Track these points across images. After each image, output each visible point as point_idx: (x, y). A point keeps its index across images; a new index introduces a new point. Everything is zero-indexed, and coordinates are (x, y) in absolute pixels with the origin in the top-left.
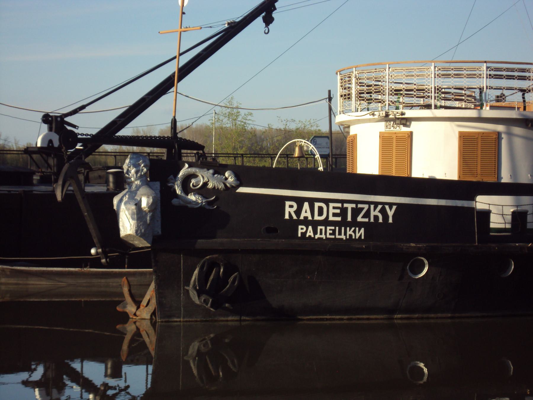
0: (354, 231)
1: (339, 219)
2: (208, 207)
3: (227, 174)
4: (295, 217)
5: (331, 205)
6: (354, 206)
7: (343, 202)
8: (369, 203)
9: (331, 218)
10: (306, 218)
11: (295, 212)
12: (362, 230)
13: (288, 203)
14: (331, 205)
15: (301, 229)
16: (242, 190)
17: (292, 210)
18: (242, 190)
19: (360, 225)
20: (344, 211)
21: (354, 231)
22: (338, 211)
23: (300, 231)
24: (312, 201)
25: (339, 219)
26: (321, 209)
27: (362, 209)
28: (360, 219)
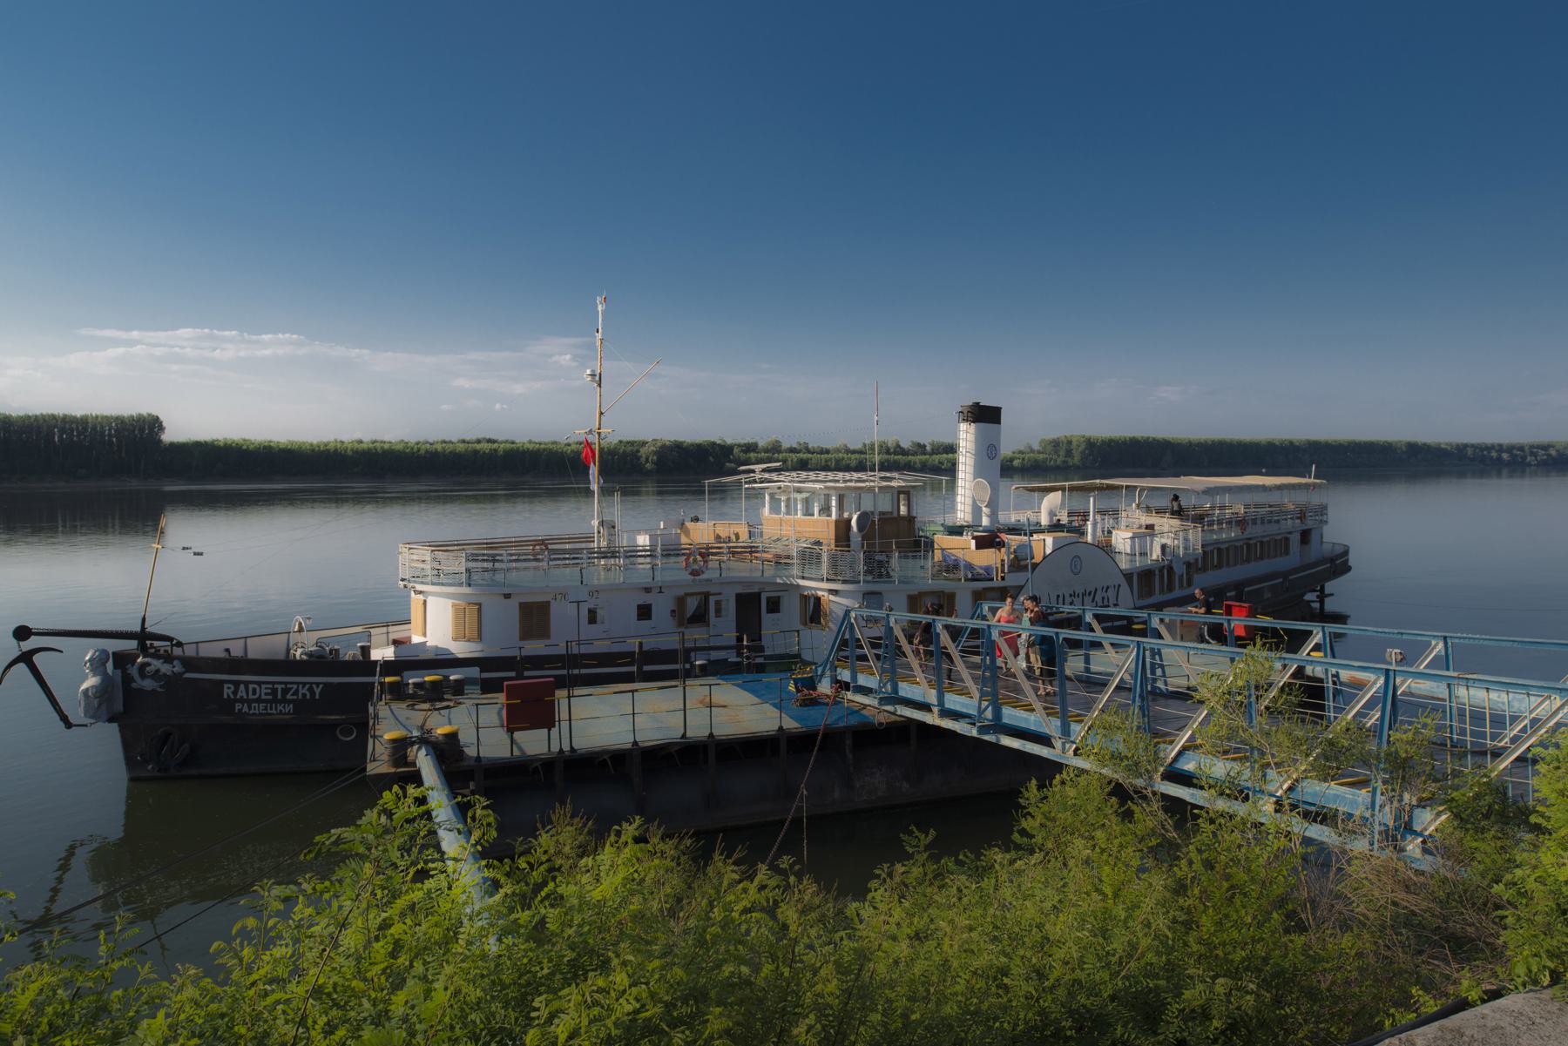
0: (284, 707)
1: (270, 697)
2: (159, 690)
3: (175, 662)
4: (232, 697)
5: (263, 686)
6: (283, 686)
7: (273, 683)
8: (298, 683)
9: (263, 697)
10: (242, 697)
11: (233, 693)
12: (291, 706)
13: (226, 686)
14: (263, 686)
15: (238, 706)
16: (187, 675)
17: (230, 691)
18: (187, 675)
19: (289, 702)
20: (274, 691)
21: (284, 707)
22: (269, 691)
23: (237, 708)
24: (247, 684)
25: (270, 697)
26: (254, 690)
27: (291, 689)
28: (289, 697)
